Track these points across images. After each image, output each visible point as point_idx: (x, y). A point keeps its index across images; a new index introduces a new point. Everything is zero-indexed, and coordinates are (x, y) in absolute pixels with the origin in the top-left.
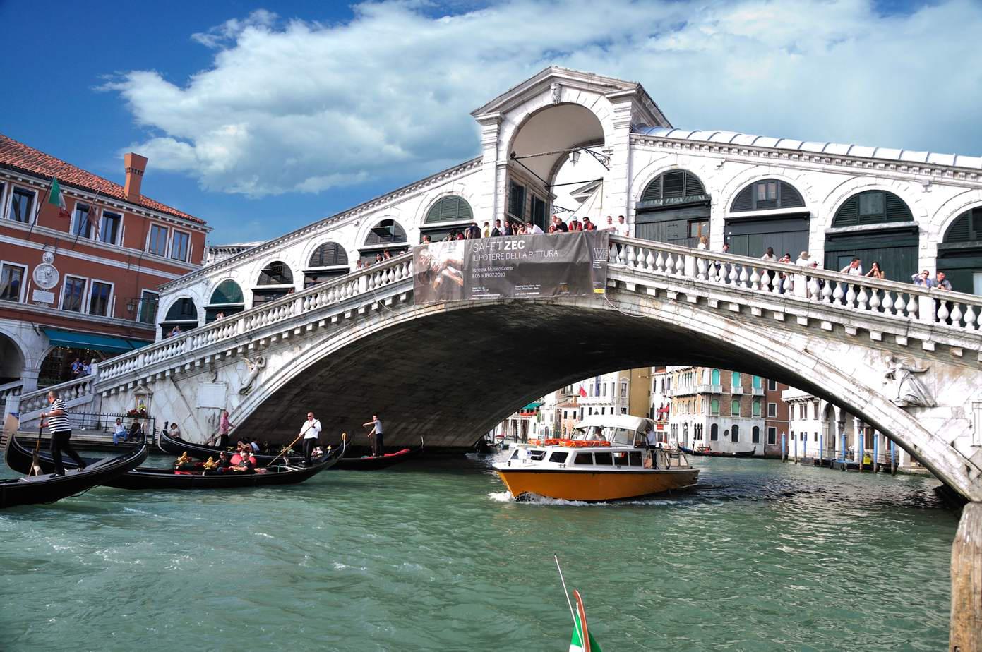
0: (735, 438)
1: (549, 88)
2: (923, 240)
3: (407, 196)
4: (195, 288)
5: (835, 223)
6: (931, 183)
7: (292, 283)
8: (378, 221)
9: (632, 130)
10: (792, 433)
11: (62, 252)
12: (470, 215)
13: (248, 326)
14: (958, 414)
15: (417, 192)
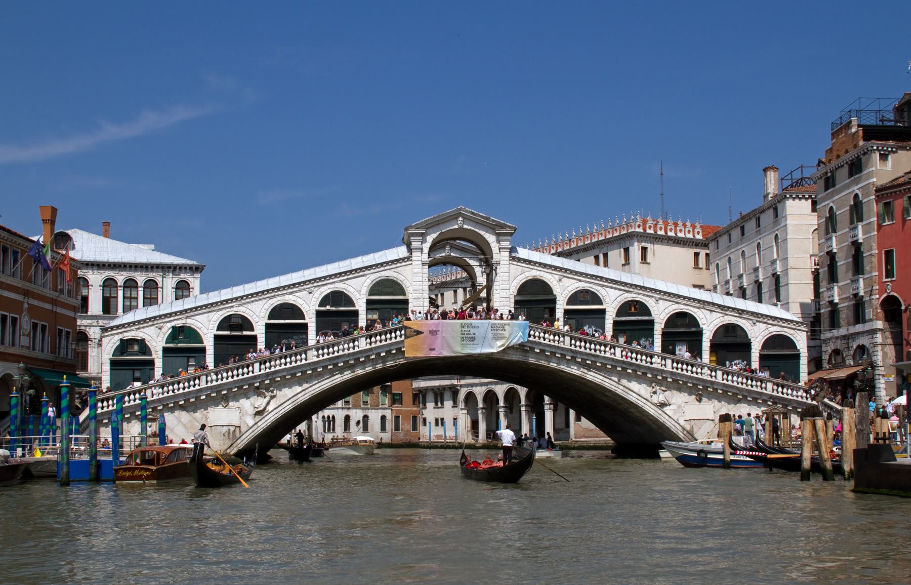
0: (366, 429)
1: (457, 218)
2: (656, 324)
3: (351, 276)
4: (146, 330)
5: (618, 314)
6: (660, 299)
7: (253, 330)
8: (329, 291)
9: (510, 253)
10: (425, 420)
11: (35, 302)
12: (404, 293)
13: (263, 366)
14: (679, 407)
15: (362, 273)
